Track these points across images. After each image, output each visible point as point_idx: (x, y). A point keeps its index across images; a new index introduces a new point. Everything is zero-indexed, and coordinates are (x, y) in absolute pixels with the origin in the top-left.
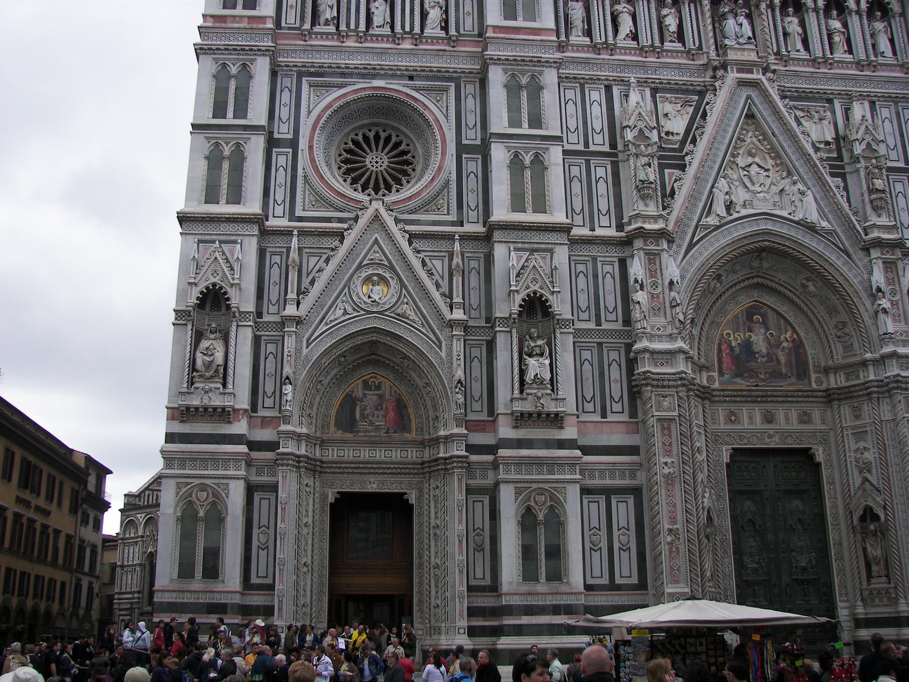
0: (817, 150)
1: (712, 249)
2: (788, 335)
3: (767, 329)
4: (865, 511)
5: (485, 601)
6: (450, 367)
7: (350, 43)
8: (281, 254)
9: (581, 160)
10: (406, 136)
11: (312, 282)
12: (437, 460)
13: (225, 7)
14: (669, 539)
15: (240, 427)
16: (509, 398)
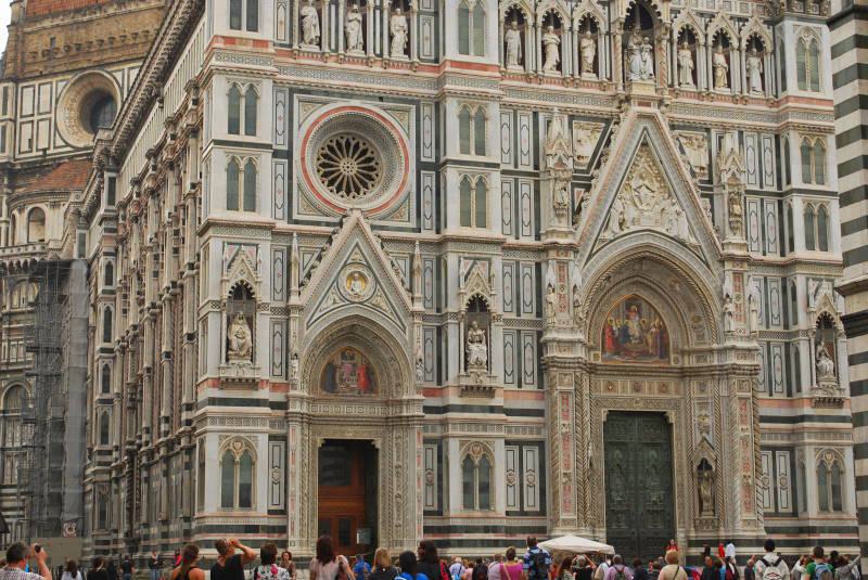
0: (693, 174)
1: (605, 259)
2: (657, 321)
3: (640, 317)
4: (702, 462)
5: (434, 522)
6: (412, 348)
7: (331, 64)
8: (282, 251)
9: (511, 178)
10: (371, 145)
11: (309, 276)
12: (401, 417)
13: (232, 28)
14: (564, 480)
15: (264, 393)
16: (456, 374)
